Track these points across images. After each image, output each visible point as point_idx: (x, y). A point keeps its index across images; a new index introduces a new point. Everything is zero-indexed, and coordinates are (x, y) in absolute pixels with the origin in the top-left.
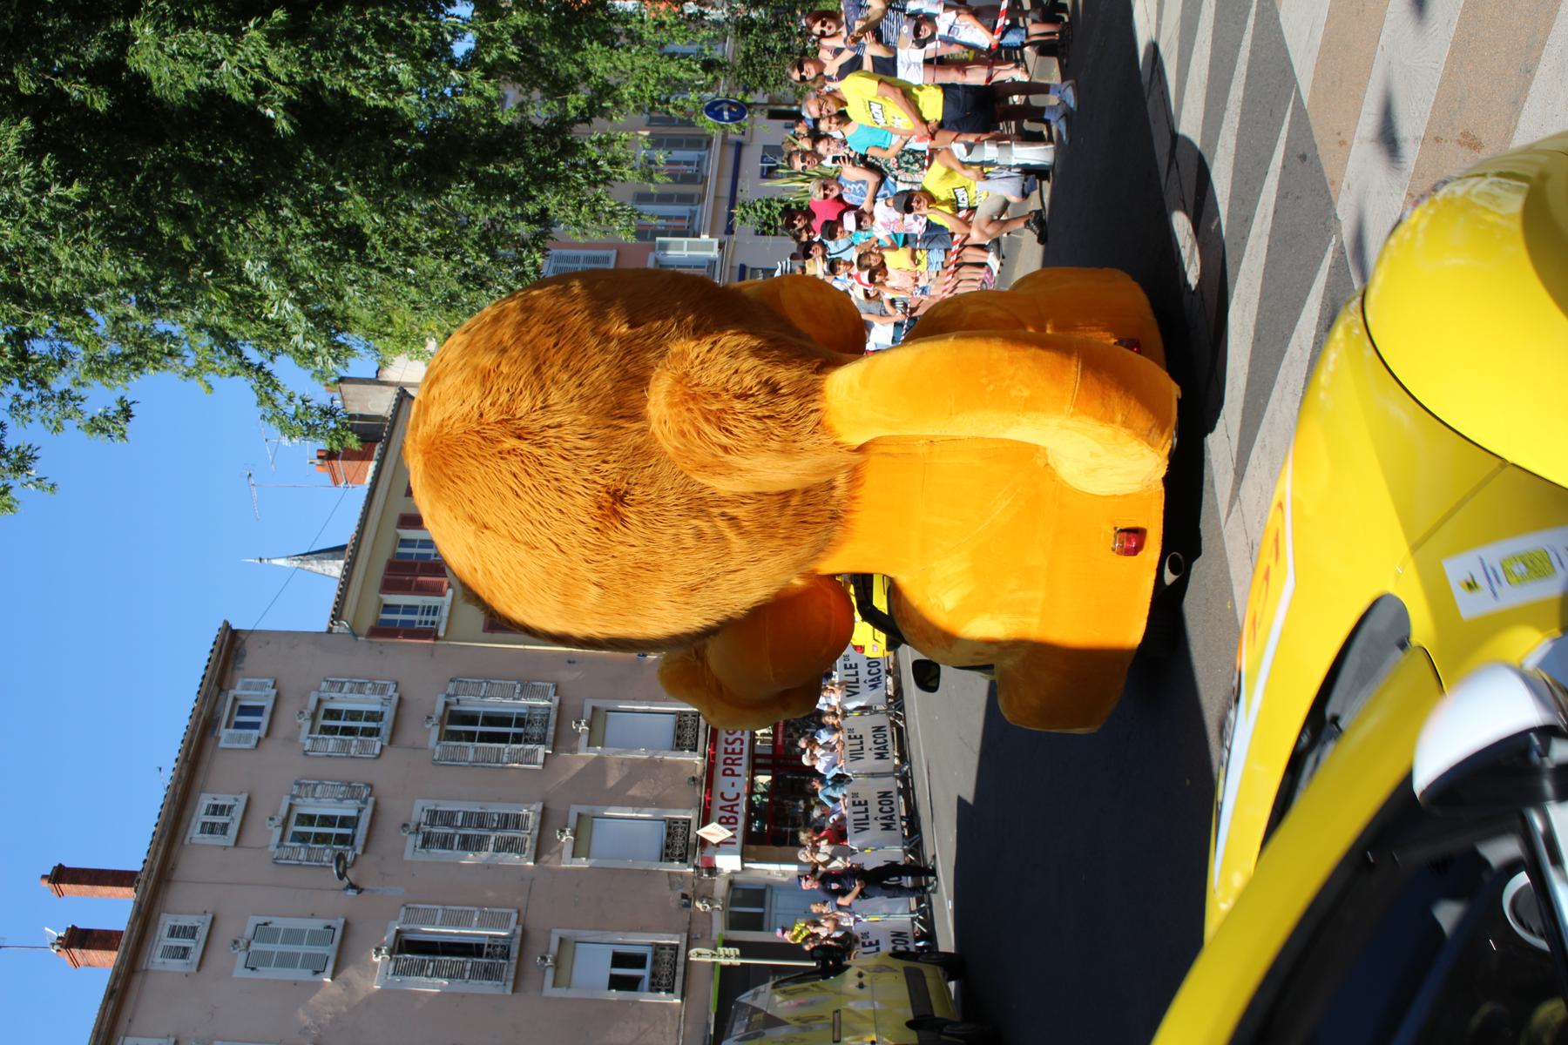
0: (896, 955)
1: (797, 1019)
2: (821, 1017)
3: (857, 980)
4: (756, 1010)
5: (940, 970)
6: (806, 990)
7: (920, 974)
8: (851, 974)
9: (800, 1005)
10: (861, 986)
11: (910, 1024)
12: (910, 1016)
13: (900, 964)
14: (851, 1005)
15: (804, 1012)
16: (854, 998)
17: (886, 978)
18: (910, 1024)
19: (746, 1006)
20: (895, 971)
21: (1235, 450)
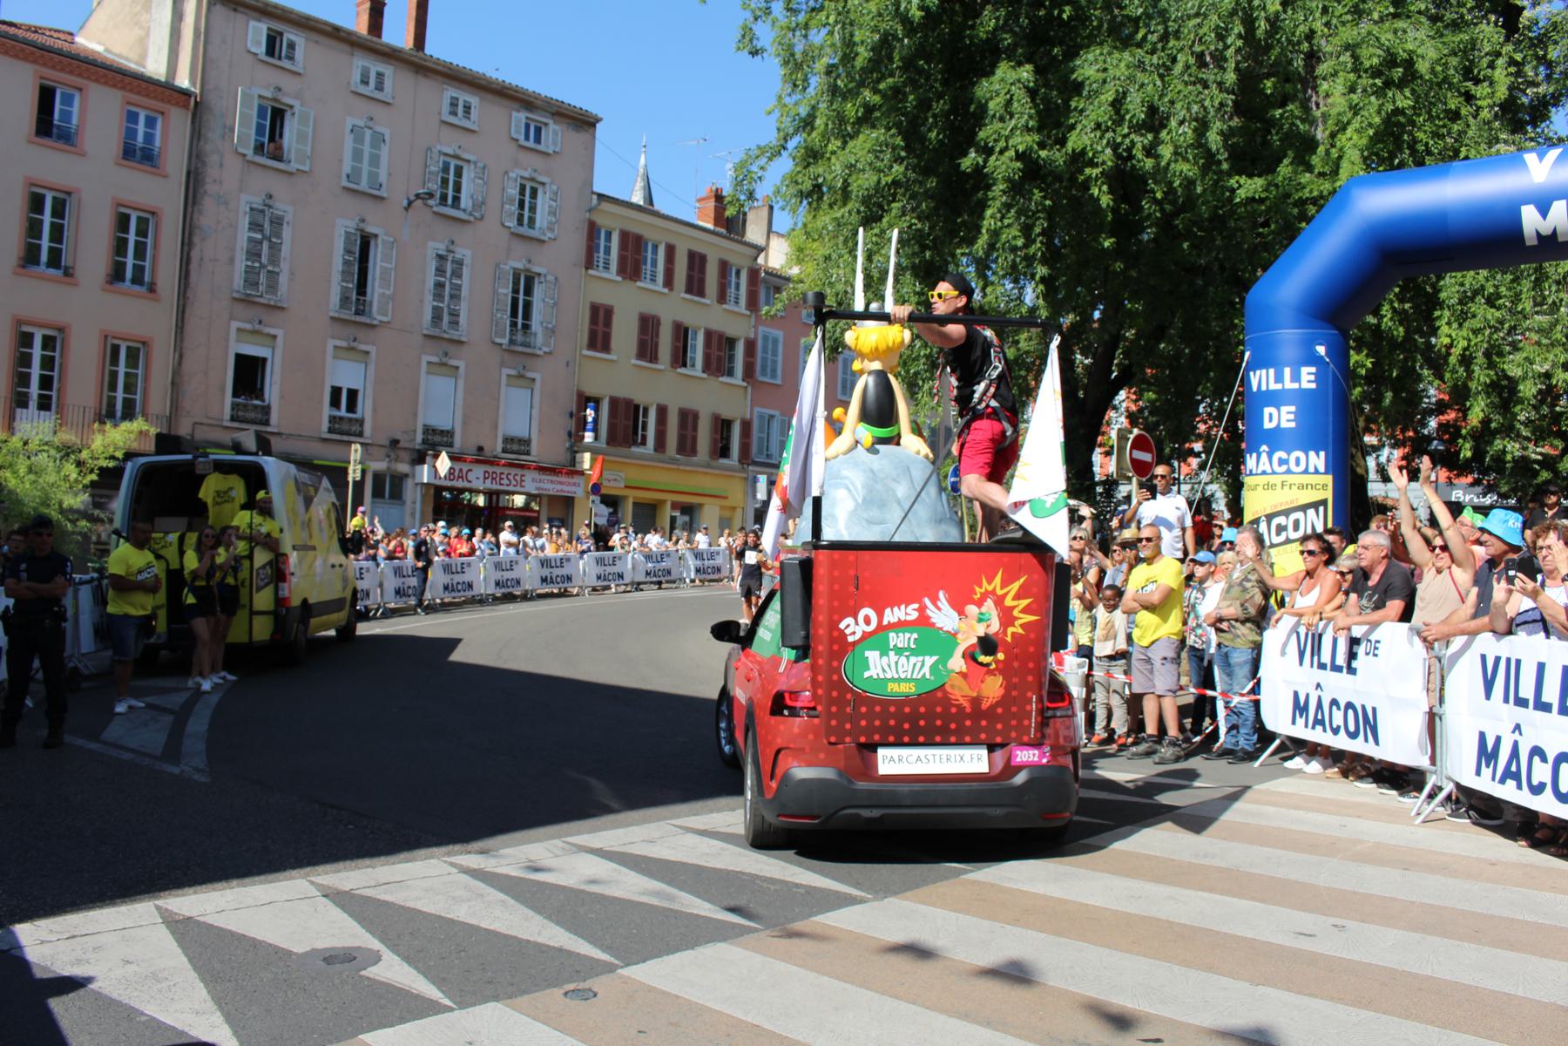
0: (355, 591)
1: (310, 520)
2: (311, 537)
3: (337, 563)
4: (317, 490)
5: (343, 623)
6: (331, 526)
7: (341, 609)
8: (341, 559)
9: (320, 522)
10: (333, 566)
11: (305, 601)
12: (311, 601)
13: (348, 594)
14: (318, 562)
15: (315, 526)
16: (325, 561)
17: (339, 585)
18: (305, 601)
19: (320, 482)
20: (344, 589)
21: (722, 830)
